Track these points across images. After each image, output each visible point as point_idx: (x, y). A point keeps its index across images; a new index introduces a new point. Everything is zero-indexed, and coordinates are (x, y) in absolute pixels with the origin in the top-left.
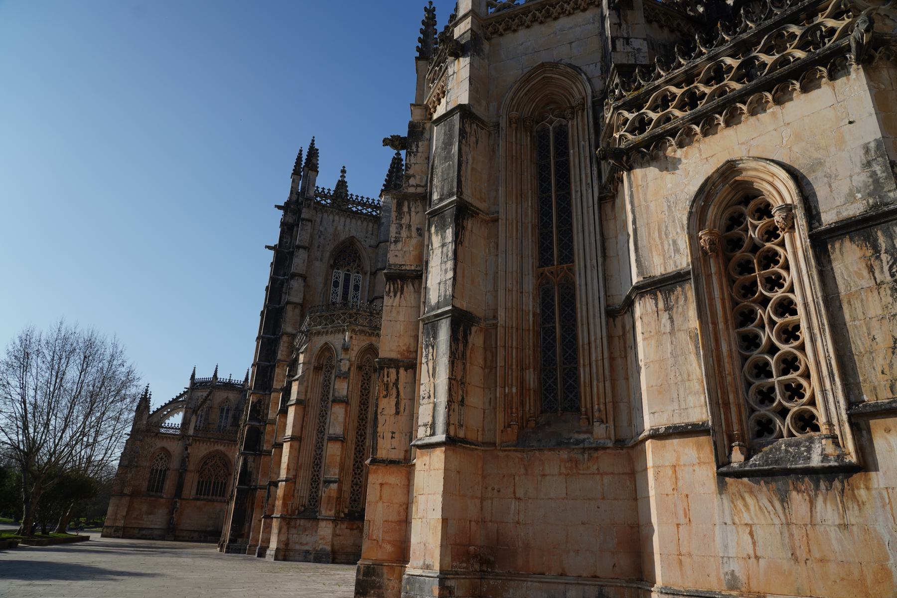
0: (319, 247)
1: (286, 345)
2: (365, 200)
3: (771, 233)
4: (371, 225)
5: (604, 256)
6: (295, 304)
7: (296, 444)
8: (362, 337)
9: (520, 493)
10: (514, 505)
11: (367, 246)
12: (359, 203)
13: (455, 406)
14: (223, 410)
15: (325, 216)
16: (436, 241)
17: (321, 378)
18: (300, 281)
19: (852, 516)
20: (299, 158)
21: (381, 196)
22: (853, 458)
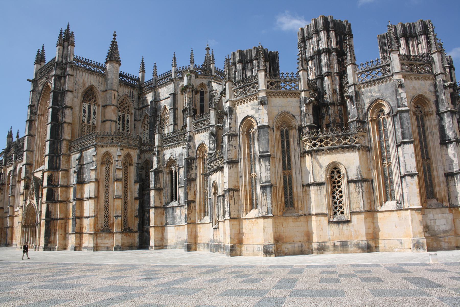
0: (76, 90)
1: (65, 145)
3: (339, 177)
4: (101, 78)
6: (69, 124)
7: (96, 200)
9: (284, 226)
10: (283, 229)
11: (99, 91)
12: (95, 66)
15: (78, 72)
16: (263, 164)
18: (70, 110)
19: (348, 228)
21: (106, 63)
22: (349, 220)
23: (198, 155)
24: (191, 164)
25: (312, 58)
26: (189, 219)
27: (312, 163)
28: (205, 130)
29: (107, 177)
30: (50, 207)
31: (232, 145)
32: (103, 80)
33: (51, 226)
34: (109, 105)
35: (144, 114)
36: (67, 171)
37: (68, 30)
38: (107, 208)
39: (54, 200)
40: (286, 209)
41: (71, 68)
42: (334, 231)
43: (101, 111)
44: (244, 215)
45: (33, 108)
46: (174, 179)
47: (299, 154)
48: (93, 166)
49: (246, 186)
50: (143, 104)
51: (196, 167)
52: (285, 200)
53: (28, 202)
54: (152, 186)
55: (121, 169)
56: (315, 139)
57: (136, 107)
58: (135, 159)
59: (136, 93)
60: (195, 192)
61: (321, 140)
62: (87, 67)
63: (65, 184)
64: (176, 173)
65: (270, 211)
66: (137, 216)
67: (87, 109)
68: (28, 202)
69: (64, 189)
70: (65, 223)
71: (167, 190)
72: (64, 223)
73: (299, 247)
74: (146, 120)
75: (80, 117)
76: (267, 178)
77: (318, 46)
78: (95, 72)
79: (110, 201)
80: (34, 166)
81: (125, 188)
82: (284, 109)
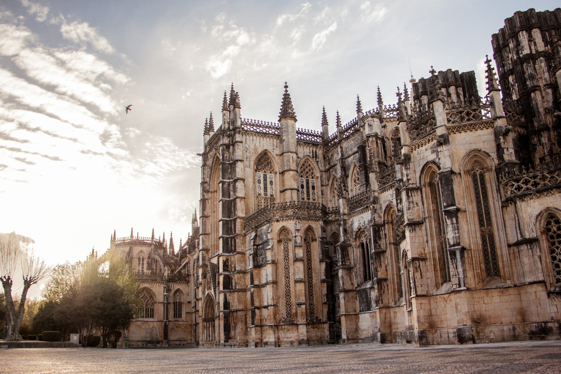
1: (240, 224)
2: (270, 124)
4: (275, 140)
5: (505, 226)
6: (241, 198)
7: (275, 286)
8: (304, 222)
9: (486, 302)
10: (484, 306)
14: (139, 259)
15: (248, 136)
16: (449, 222)
17: (282, 247)
18: (241, 182)
20: (225, 98)
21: (279, 121)
23: (386, 219)
24: (379, 231)
25: (511, 72)
26: (380, 302)
27: (517, 213)
28: (391, 187)
29: (286, 258)
30: (229, 298)
31: (413, 202)
32: (278, 141)
33: (231, 319)
34: (287, 171)
35: (332, 177)
36: (243, 254)
37: (232, 91)
38: (288, 295)
39: (232, 289)
40: (488, 279)
42: (558, 307)
43: (278, 179)
44: (434, 291)
45: (206, 185)
46: (366, 253)
47: (500, 203)
48: (268, 245)
49: (434, 252)
50: (329, 164)
51: (385, 235)
52: (486, 267)
53: (207, 292)
55: (301, 246)
57: (323, 169)
58: (318, 233)
59: (320, 152)
60: (386, 267)
61: (526, 180)
63: (243, 269)
64: (367, 245)
66: (325, 303)
67: (262, 179)
68: (207, 292)
69: (241, 275)
70: (246, 315)
71: (359, 268)
72: (244, 315)
73: (509, 330)
74: (335, 183)
75: (255, 189)
77: (517, 53)
78: (267, 134)
79: (291, 286)
80: (210, 251)
81: (309, 269)
82: (474, 147)
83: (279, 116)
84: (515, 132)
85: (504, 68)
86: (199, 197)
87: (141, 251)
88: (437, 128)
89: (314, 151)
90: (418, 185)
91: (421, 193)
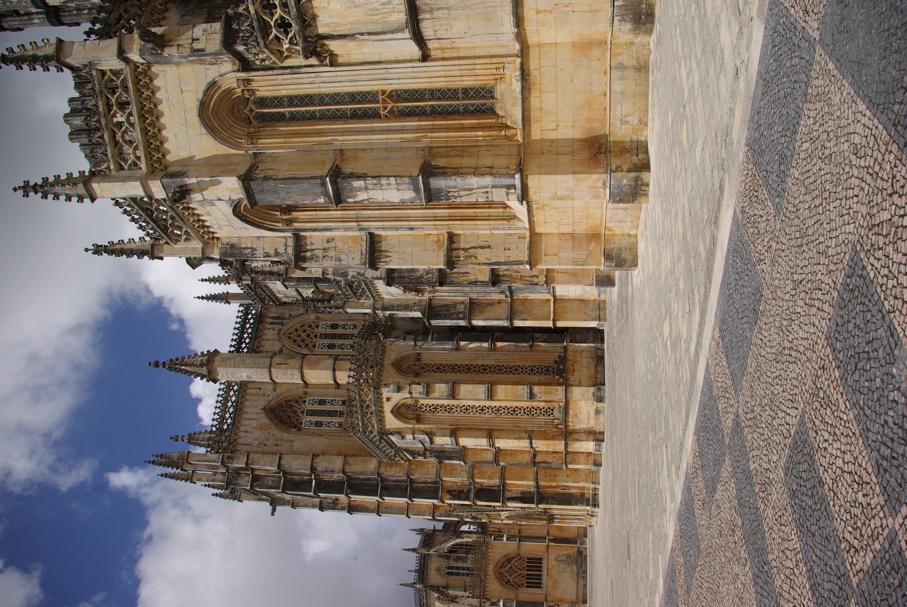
1: (389, 468)
4: (249, 391)
7: (495, 434)
8: (385, 374)
12: (225, 405)
13: (494, 171)
14: (449, 574)
15: (240, 441)
16: (362, 196)
18: (317, 460)
21: (215, 381)
26: (535, 280)
31: (325, 249)
32: (251, 386)
39: (499, 486)
41: (232, 459)
45: (325, 504)
49: (436, 219)
53: (503, 517)
54: (462, 323)
56: (265, 29)
62: (229, 421)
65: (508, 181)
69: (476, 471)
76: (403, 187)
78: (237, 405)
83: (208, 381)
84: (167, 10)
85: (32, 14)
86: (345, 514)
87: (438, 570)
88: (151, 197)
89: (271, 321)
90: (290, 234)
91: (306, 230)
